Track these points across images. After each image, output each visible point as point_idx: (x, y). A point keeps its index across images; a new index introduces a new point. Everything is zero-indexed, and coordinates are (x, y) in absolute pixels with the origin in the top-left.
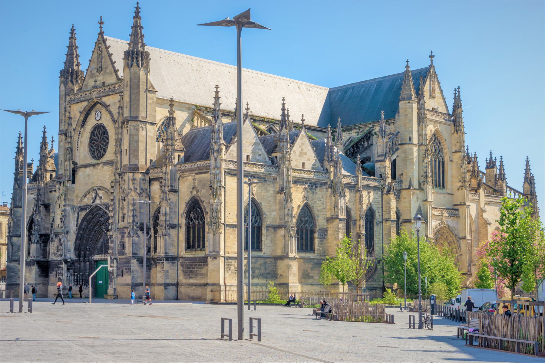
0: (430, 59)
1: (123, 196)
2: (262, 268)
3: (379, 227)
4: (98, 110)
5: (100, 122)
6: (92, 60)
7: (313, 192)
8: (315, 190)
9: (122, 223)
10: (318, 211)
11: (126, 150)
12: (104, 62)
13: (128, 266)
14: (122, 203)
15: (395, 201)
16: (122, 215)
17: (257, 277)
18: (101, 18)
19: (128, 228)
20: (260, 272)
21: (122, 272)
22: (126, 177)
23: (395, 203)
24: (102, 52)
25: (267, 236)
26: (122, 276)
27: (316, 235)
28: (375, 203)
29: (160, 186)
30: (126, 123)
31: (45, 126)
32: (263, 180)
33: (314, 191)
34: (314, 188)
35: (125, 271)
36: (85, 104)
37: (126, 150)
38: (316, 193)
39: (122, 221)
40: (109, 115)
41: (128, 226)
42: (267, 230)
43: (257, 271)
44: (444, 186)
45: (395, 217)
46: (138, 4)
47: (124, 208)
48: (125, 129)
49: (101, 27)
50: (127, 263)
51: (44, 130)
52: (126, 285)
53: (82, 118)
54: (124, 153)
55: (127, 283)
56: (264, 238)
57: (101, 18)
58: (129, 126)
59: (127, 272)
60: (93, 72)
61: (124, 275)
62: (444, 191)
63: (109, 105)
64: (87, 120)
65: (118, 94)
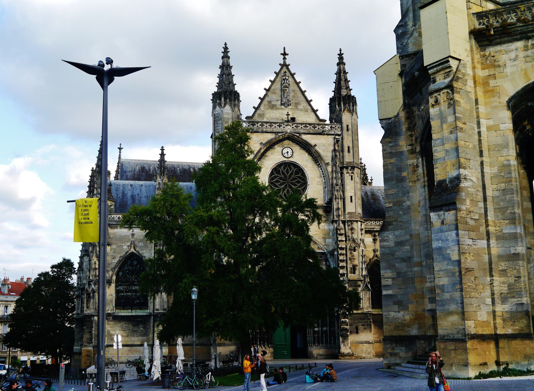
1: (353, 245)
4: (286, 146)
5: (291, 159)
6: (271, 90)
9: (352, 275)
11: (351, 197)
12: (294, 97)
13: (367, 322)
14: (351, 253)
16: (351, 266)
18: (284, 49)
19: (362, 280)
21: (357, 329)
22: (355, 225)
24: (289, 85)
26: (357, 333)
29: (373, 239)
30: (350, 168)
31: (162, 147)
35: (361, 327)
36: (270, 136)
37: (351, 197)
39: (351, 273)
40: (307, 154)
41: (362, 279)
46: (340, 50)
47: (354, 259)
48: (348, 175)
49: (285, 58)
50: (364, 319)
51: (162, 153)
52: (366, 343)
53: (262, 151)
54: (348, 200)
55: (360, 340)
57: (284, 49)
58: (355, 172)
59: (365, 329)
60: (273, 103)
61: (360, 332)
63: (316, 145)
64: (267, 154)
65: (333, 136)
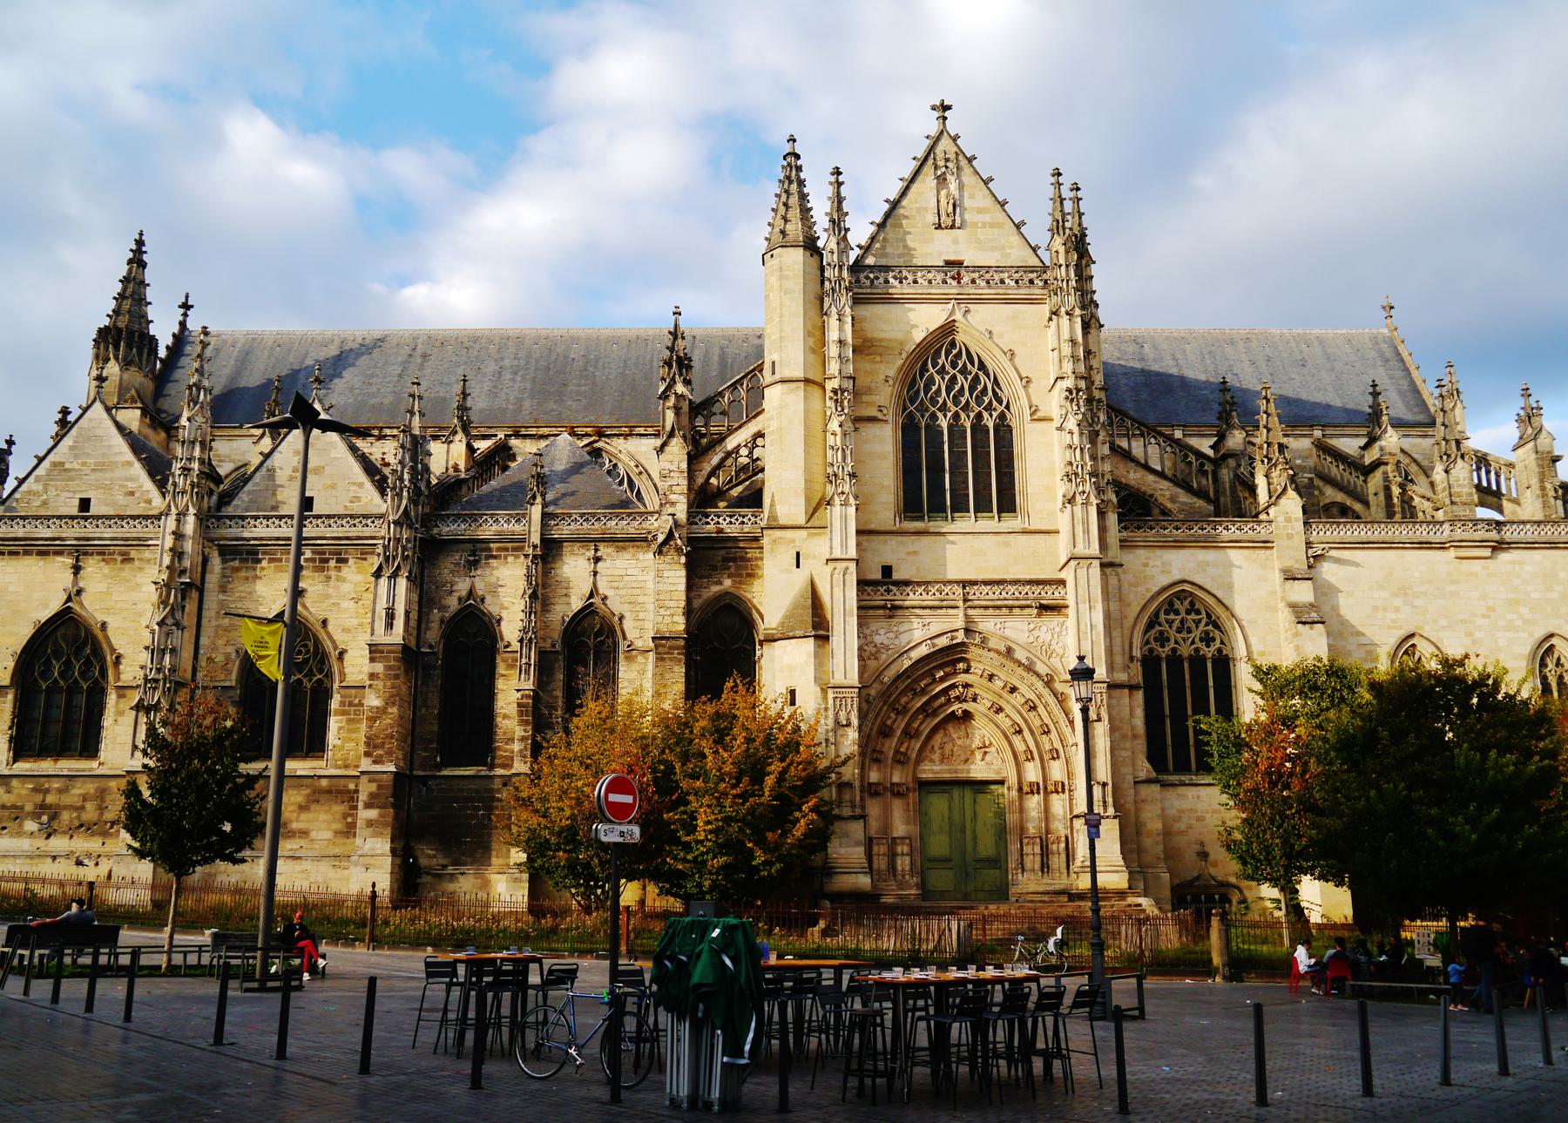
0: (936, 114)
2: (90, 806)
3: (635, 667)
7: (329, 578)
8: (338, 569)
10: (346, 630)
15: (683, 573)
17: (64, 833)
20: (79, 818)
23: (684, 580)
25: (120, 713)
27: (335, 703)
28: (623, 592)
32: (119, 558)
33: (333, 573)
34: (332, 563)
38: (344, 580)
42: (120, 696)
43: (66, 816)
44: (1008, 504)
45: (682, 627)
56: (107, 721)
62: (1010, 523)
